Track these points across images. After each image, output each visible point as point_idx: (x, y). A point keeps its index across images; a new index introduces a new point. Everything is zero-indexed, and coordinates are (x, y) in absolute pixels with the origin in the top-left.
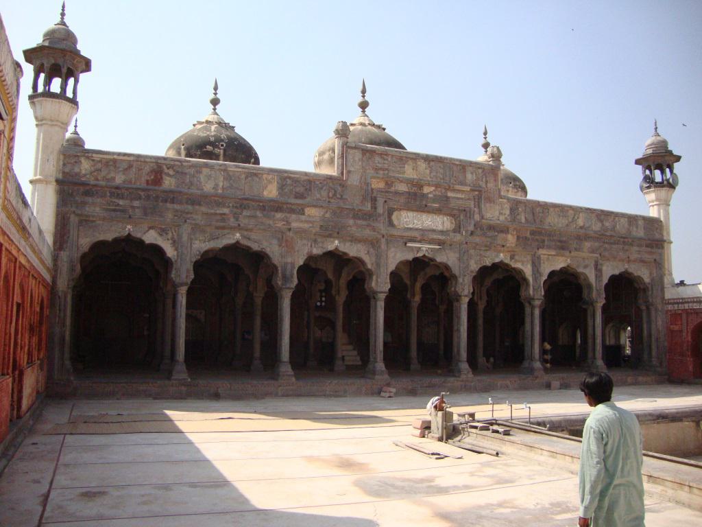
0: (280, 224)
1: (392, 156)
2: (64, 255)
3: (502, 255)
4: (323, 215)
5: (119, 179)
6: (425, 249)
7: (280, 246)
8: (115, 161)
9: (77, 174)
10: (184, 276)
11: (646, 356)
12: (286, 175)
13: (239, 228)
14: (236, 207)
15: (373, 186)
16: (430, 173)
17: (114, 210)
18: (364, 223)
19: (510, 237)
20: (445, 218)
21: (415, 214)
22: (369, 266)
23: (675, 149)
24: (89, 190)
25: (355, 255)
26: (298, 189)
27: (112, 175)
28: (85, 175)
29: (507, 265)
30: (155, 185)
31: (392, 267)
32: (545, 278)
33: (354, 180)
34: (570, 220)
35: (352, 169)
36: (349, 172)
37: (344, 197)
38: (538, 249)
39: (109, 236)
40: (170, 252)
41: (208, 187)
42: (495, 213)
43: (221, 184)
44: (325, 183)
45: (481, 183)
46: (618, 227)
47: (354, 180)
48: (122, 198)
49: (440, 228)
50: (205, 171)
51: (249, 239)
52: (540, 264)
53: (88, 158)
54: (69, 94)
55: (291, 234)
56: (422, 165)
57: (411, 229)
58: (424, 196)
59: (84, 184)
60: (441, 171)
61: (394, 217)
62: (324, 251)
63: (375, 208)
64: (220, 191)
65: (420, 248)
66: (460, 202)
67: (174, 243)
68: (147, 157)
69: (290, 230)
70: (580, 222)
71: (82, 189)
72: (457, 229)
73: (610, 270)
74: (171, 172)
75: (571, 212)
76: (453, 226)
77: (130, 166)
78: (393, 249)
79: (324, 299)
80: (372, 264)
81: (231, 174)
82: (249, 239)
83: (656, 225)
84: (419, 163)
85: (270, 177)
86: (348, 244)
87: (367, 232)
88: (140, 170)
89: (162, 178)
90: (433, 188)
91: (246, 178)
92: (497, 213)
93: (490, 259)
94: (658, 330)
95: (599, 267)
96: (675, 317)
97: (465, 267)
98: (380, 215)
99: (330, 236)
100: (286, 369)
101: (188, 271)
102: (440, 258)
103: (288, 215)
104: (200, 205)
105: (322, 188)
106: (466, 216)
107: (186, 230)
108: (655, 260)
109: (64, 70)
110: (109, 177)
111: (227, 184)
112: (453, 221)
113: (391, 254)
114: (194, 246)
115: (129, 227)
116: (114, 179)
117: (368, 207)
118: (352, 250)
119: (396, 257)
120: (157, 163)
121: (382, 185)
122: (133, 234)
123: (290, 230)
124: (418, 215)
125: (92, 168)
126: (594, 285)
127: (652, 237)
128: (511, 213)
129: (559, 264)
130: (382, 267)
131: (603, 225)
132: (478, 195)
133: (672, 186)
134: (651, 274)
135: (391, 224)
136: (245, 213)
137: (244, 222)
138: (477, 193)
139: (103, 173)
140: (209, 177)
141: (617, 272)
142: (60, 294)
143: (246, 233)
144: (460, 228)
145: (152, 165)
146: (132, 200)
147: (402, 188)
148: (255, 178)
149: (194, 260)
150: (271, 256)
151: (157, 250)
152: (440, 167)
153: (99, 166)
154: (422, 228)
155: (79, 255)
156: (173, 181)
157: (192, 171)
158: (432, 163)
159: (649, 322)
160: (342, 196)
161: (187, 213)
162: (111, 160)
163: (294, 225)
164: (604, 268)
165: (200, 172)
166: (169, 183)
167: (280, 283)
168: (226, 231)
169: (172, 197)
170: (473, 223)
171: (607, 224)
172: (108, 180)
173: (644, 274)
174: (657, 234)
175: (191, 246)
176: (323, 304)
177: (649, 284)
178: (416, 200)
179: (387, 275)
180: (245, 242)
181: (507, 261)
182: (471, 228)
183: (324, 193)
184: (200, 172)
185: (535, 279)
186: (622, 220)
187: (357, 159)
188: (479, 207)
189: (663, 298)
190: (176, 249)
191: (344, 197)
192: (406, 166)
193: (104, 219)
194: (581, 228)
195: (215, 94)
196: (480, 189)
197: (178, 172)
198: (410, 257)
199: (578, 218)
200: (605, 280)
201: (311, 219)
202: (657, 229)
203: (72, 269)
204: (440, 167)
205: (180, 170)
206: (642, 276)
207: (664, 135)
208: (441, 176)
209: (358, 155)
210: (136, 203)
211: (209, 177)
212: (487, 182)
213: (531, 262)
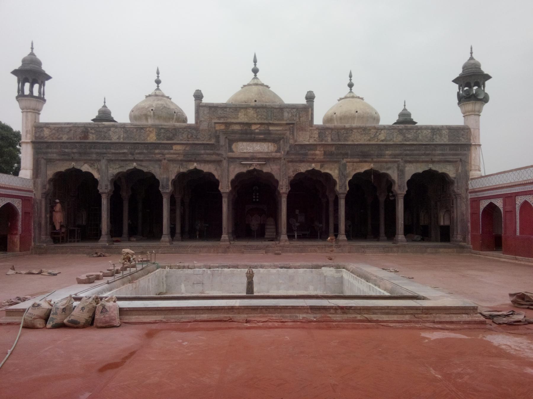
0: (158, 156)
1: (230, 108)
2: (39, 181)
3: (313, 165)
4: (184, 150)
5: (65, 139)
6: (255, 165)
7: (160, 168)
8: (62, 128)
9: (42, 137)
10: (104, 188)
11: (455, 233)
12: (160, 127)
13: (134, 160)
14: (132, 149)
15: (217, 128)
16: (257, 116)
17: (64, 155)
18: (212, 152)
19: (317, 152)
20: (270, 144)
21: (248, 143)
22: (217, 177)
23: (485, 69)
24: (49, 145)
25: (207, 171)
26: (168, 135)
27: (61, 136)
28: (46, 137)
29: (319, 172)
30: (85, 139)
31: (232, 177)
32: (350, 178)
33: (204, 126)
34: (373, 136)
35: (202, 119)
36: (201, 121)
37: (198, 137)
38: (343, 159)
39: (63, 169)
40: (96, 176)
41: (115, 139)
42: (304, 139)
43: (122, 136)
44: (185, 130)
45: (295, 119)
46: (420, 137)
47: (204, 126)
48: (67, 148)
49: (266, 150)
50: (112, 129)
51: (141, 166)
52: (345, 169)
53: (47, 127)
54: (36, 93)
55: (166, 161)
56: (251, 112)
57: (245, 153)
58: (252, 133)
59: (46, 142)
60: (265, 114)
61: (234, 147)
62: (187, 170)
63: (219, 142)
64: (122, 140)
65: (251, 164)
66: (279, 132)
67: (98, 170)
68: (80, 123)
69: (165, 159)
70: (382, 137)
71: (45, 145)
72: (278, 151)
73: (411, 170)
74: (93, 132)
75: (373, 131)
76: (276, 149)
77: (71, 130)
78: (232, 166)
79: (258, 197)
80: (219, 176)
81: (128, 129)
82: (141, 166)
83: (462, 132)
84: (249, 111)
85: (151, 129)
86: (202, 165)
87: (214, 157)
88: (76, 132)
89: (88, 135)
90: (259, 126)
91: (137, 130)
92: (308, 137)
93: (303, 168)
94: (463, 214)
95: (400, 168)
96: (476, 201)
97: (283, 176)
98: (222, 146)
99: (190, 161)
100: (166, 238)
101: (107, 186)
102: (265, 170)
103: (163, 151)
104: (110, 149)
105: (183, 133)
106: (284, 141)
107: (103, 162)
108: (461, 160)
109: (31, 80)
110: (59, 137)
111: (125, 135)
112: (276, 145)
113: (231, 169)
114: (110, 172)
115: (73, 163)
116: (61, 138)
117: (213, 141)
118: (206, 168)
119: (235, 170)
120: (84, 127)
121: (223, 127)
122: (76, 167)
123: (165, 159)
124: (251, 144)
125: (51, 133)
126: (396, 182)
127: (459, 143)
128: (319, 136)
129: (364, 168)
130: (226, 178)
131: (405, 137)
132: (293, 127)
133: (486, 99)
134: (457, 171)
135: (231, 151)
136: (137, 151)
137: (137, 157)
138: (291, 126)
139: (56, 136)
140: (114, 132)
141: (420, 171)
142: (38, 201)
143: (139, 163)
144: (280, 149)
145: (82, 128)
146: (72, 149)
147: (237, 127)
148: (142, 131)
149: (110, 179)
150: (155, 174)
151: (89, 175)
152: (264, 112)
153: (54, 131)
154: (251, 149)
155: (48, 180)
156: (94, 136)
157: (105, 130)
158: (258, 110)
159: (457, 209)
160: (196, 136)
161: (104, 154)
162: (60, 128)
163: (167, 156)
164: (407, 169)
165: (110, 130)
166: (92, 138)
167: (160, 190)
168: (128, 163)
169: (94, 145)
170: (289, 145)
171: (409, 136)
172: (59, 139)
173: (450, 171)
174: (463, 140)
175: (108, 172)
176: (257, 200)
177: (455, 178)
178: (248, 134)
179: (228, 182)
180: (139, 168)
181: (318, 168)
182: (287, 149)
183: (185, 136)
184: (110, 130)
185: (341, 180)
186: (425, 131)
187: (205, 112)
188: (293, 135)
189: (467, 190)
190: (100, 174)
191: (198, 137)
192: (240, 114)
193: (59, 160)
194: (382, 141)
195: (158, 77)
196: (293, 122)
197: (97, 131)
198: (244, 170)
199: (380, 134)
200: (408, 177)
201: (177, 152)
202: (463, 135)
203: (44, 187)
204: (264, 112)
205: (98, 130)
206: (448, 173)
207: (477, 58)
208: (265, 117)
209: (206, 111)
210: (75, 150)
211: (114, 132)
212: (300, 117)
213: (338, 168)
